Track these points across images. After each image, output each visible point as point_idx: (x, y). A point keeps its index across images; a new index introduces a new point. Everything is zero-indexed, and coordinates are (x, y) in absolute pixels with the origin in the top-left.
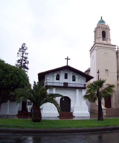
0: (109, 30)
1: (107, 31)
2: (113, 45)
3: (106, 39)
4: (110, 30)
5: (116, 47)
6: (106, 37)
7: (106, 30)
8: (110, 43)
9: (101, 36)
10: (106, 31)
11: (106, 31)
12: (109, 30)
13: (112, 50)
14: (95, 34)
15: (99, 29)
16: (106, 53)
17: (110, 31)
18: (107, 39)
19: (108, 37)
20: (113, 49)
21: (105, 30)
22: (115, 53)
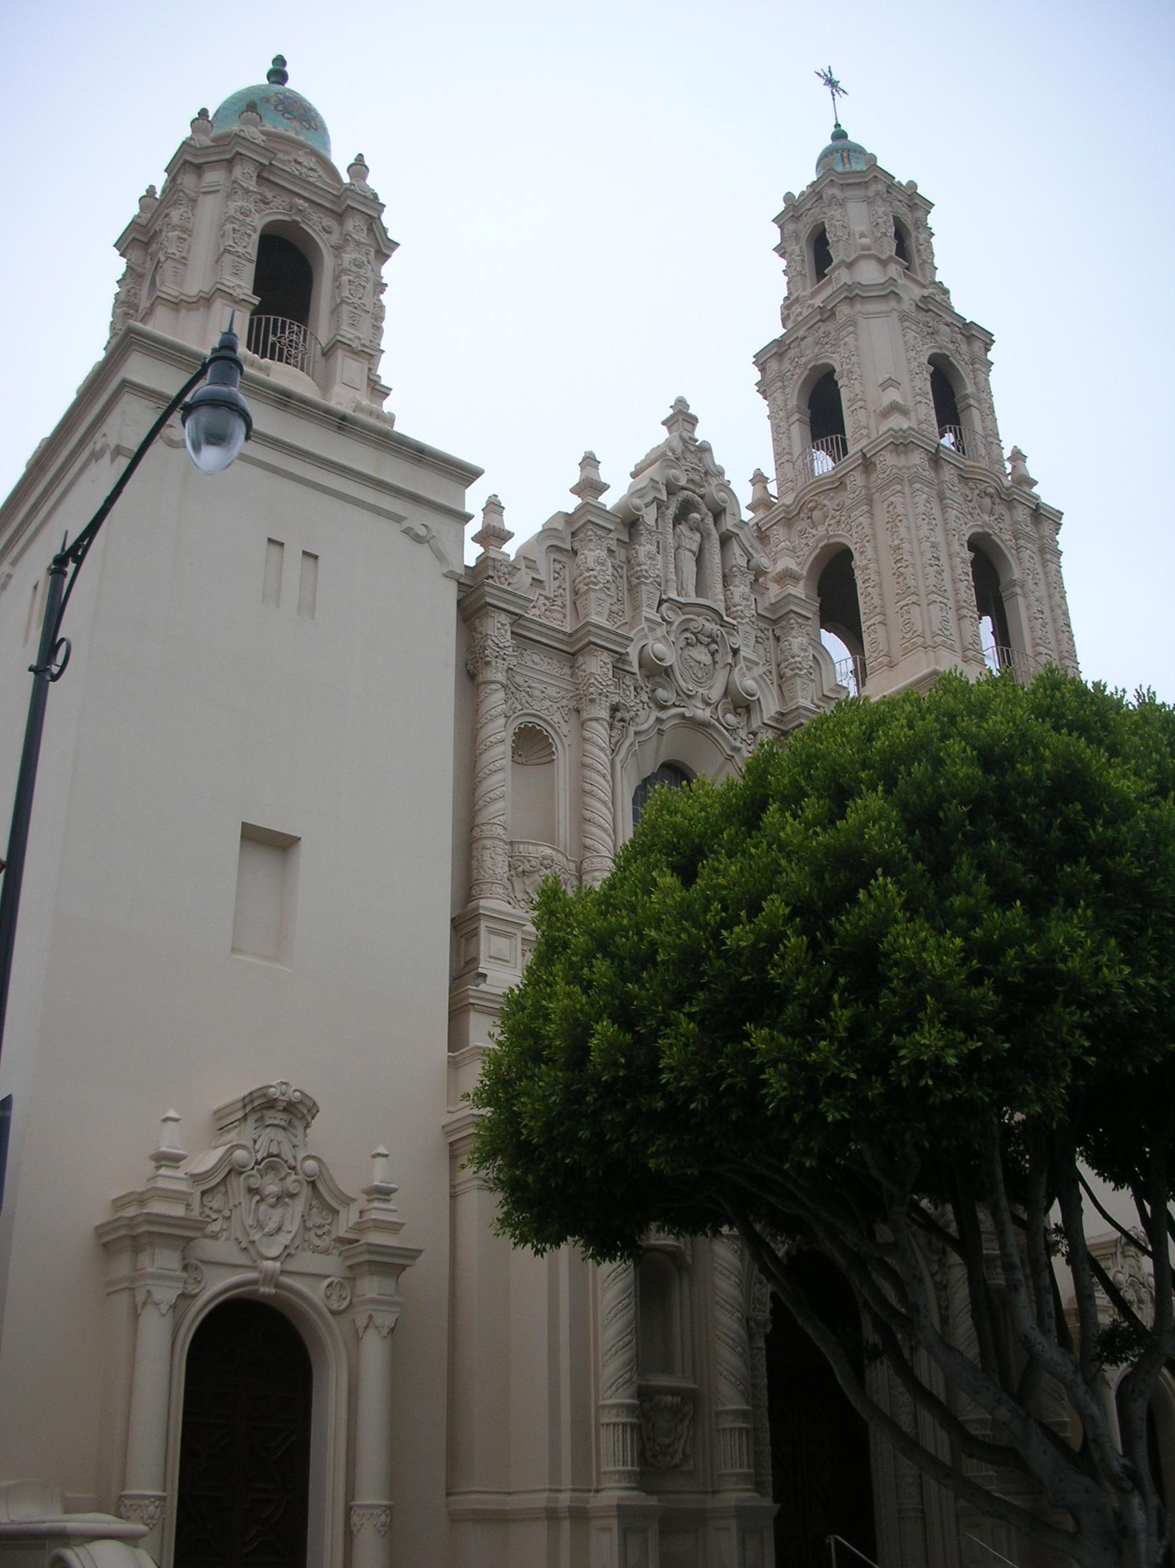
0: (383, 257)
1: (338, 249)
2: (418, 454)
3: (315, 351)
4: (396, 255)
5: (474, 499)
6: (322, 328)
7: (327, 222)
8: (371, 413)
9: (243, 283)
10: (335, 239)
11: (324, 243)
12: (383, 248)
13: (392, 530)
14: (131, 277)
15: (214, 177)
16: (293, 552)
17: (389, 271)
18: (327, 353)
19: (347, 332)
20: (417, 518)
21: (316, 226)
22: (450, 595)
